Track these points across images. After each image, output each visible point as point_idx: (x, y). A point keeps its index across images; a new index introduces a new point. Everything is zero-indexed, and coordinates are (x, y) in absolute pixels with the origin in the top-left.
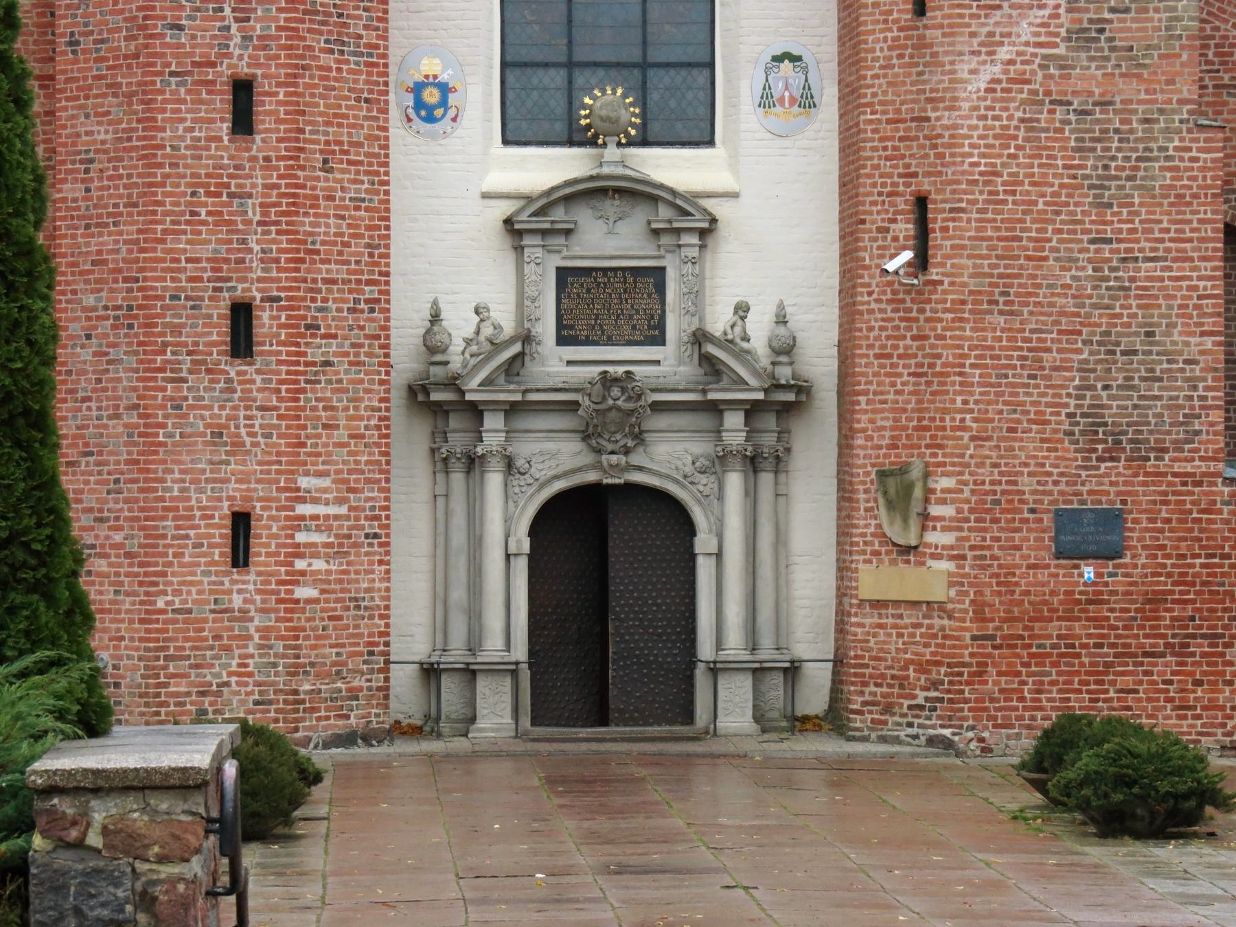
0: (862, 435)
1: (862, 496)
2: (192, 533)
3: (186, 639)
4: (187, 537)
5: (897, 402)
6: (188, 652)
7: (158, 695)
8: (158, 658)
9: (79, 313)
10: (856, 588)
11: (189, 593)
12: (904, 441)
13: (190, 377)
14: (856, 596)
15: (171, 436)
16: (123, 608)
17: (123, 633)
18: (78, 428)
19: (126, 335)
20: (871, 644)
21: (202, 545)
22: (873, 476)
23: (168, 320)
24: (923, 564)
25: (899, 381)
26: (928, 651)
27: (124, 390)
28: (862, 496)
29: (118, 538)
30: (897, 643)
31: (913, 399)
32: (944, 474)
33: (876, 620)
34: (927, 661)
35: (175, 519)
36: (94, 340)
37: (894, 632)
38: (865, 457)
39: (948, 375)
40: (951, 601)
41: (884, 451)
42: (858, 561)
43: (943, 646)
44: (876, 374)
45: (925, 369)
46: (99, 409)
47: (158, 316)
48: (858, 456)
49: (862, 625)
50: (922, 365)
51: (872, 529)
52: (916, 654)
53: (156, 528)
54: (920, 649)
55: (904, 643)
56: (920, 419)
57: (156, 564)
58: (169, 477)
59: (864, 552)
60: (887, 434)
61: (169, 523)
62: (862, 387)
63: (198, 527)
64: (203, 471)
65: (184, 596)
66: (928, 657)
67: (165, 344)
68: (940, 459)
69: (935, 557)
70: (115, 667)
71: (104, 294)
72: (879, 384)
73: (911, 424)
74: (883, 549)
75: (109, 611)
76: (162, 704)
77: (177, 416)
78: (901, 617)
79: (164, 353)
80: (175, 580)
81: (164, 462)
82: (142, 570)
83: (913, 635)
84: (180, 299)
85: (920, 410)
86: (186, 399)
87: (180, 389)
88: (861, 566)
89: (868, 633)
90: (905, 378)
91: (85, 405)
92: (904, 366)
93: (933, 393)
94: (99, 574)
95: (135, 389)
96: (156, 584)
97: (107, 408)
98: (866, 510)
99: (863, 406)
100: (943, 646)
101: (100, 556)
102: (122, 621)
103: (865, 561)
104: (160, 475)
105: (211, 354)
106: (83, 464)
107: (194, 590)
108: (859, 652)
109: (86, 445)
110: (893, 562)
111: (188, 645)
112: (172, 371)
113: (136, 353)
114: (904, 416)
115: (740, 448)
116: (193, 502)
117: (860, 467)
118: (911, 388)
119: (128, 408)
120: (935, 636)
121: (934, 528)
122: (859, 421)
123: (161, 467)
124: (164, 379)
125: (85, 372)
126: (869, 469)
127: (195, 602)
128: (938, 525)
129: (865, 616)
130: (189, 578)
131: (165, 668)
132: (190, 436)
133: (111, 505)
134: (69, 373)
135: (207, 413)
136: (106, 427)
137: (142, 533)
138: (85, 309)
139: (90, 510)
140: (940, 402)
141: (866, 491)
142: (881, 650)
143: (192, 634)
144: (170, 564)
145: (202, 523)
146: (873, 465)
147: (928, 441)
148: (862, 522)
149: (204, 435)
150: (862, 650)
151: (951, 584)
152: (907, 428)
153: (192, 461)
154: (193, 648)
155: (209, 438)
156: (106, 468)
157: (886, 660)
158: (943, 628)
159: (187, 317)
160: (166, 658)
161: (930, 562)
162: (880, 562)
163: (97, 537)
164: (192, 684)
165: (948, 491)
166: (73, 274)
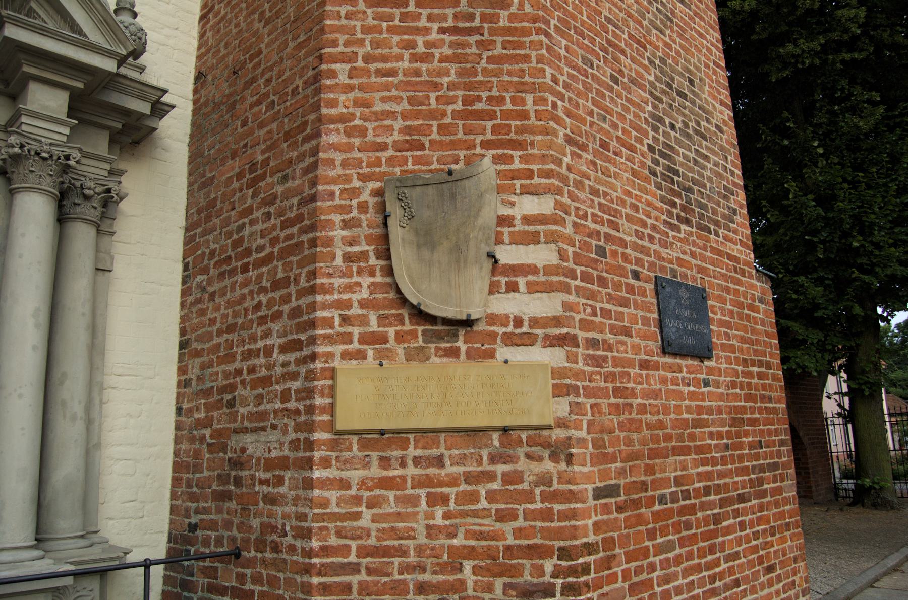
0: (341, 126)
1: (339, 233)
5: (418, 73)
10: (331, 409)
12: (435, 136)
14: (331, 426)
20: (365, 522)
22: (365, 196)
24: (491, 354)
25: (420, 40)
26: (508, 528)
28: (339, 233)
30: (430, 516)
31: (453, 68)
32: (527, 191)
33: (376, 471)
34: (508, 548)
37: (422, 492)
38: (345, 164)
39: (526, 32)
40: (562, 423)
41: (390, 152)
42: (330, 356)
43: (546, 515)
44: (366, 30)
45: (477, 23)
48: (331, 162)
49: (344, 484)
50: (471, 17)
51: (365, 294)
52: (480, 536)
54: (488, 524)
55: (446, 516)
56: (467, 101)
59: (347, 338)
60: (398, 124)
62: (341, 49)
66: (511, 541)
68: (517, 165)
69: (511, 340)
72: (376, 44)
73: (450, 109)
74: (391, 332)
78: (439, 462)
83: (473, 497)
85: (468, 87)
88: (337, 363)
89: (357, 500)
90: (434, 36)
92: (430, 18)
93: (490, 60)
98: (348, 258)
99: (343, 79)
100: (546, 515)
103: (346, 355)
108: (333, 541)
110: (416, 355)
114: (433, 95)
115: (56, 151)
117: (334, 181)
118: (447, 51)
120: (528, 497)
121: (512, 288)
122: (333, 104)
126: (356, 183)
128: (522, 281)
129: (347, 464)
140: (510, 73)
141: (346, 224)
142: (394, 533)
146: (364, 178)
147: (489, 136)
148: (338, 282)
150: (339, 534)
151: (560, 391)
152: (444, 114)
157: (403, 552)
158: (544, 480)
161: (503, 352)
162: (383, 357)
165: (542, 219)
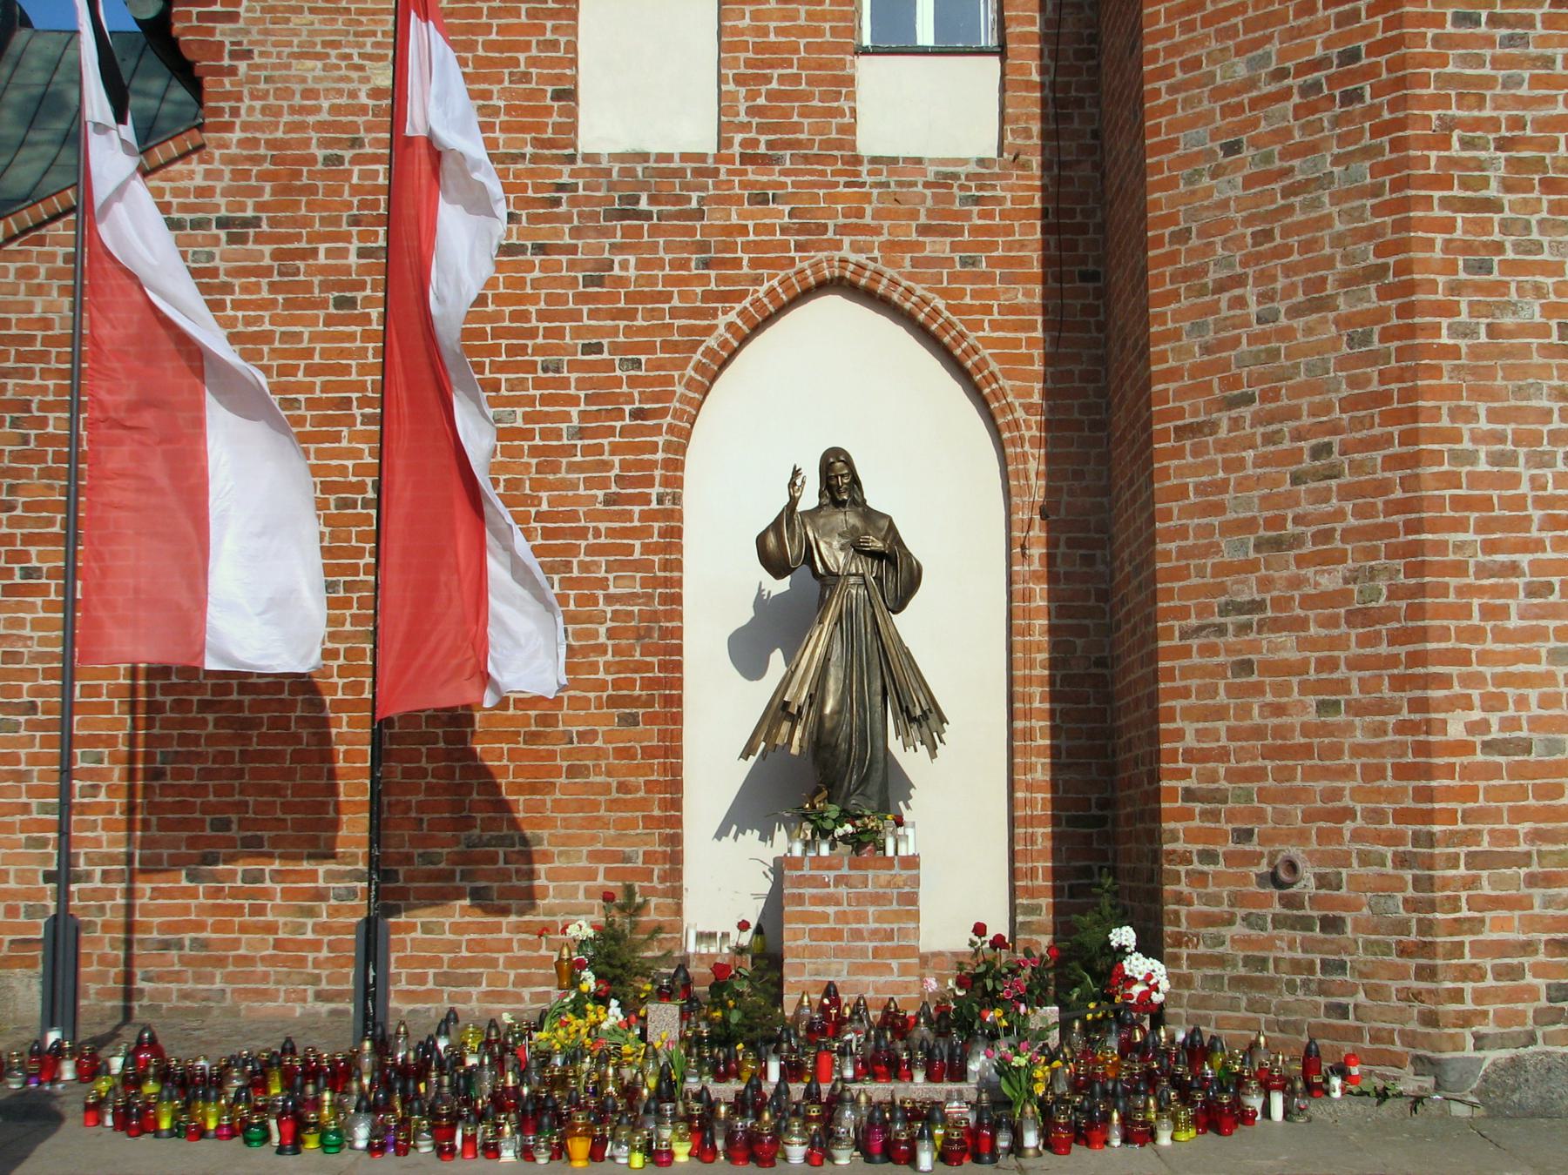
2: (1524, 559)
3: (1519, 815)
4: (1514, 569)
6: (1523, 847)
7: (1457, 950)
8: (1453, 861)
9: (1206, 105)
11: (1522, 702)
13: (1507, 198)
15: (1468, 332)
16: (1347, 742)
17: (1347, 802)
18: (1207, 349)
19: (1336, 122)
21: (1549, 588)
23: (1450, 69)
27: (1338, 240)
29: (1329, 580)
35: (1483, 527)
36: (1248, 153)
46: (1264, 297)
47: (1427, 60)
53: (1441, 547)
57: (1444, 634)
58: (1465, 429)
61: (1469, 536)
63: (1539, 545)
64: (1546, 415)
65: (1511, 712)
67: (1449, 125)
70: (1322, 881)
71: (1273, 47)
75: (1307, 751)
76: (1465, 973)
77: (1478, 288)
79: (1445, 143)
80: (1488, 671)
81: (1455, 392)
82: (1402, 650)
84: (1478, 23)
86: (1499, 248)
87: (1485, 227)
91: (1225, 297)
94: (1270, 668)
95: (1371, 233)
96: (1445, 681)
97: (1289, 291)
101: (1276, 625)
102: (1347, 772)
104: (1445, 422)
105: (1555, 147)
106: (1225, 425)
107: (1533, 695)
109: (1235, 382)
111: (1524, 827)
112: (1464, 185)
113: (1367, 152)
116: (1525, 488)
119: (1347, 281)
123: (1445, 406)
124: (1446, 203)
125: (1224, 226)
127: (1535, 723)
130: (1521, 668)
131: (1472, 883)
132: (1511, 334)
133: (1305, 507)
134: (1182, 236)
135: (1549, 281)
136: (1286, 334)
137: (1399, 563)
138: (1219, 93)
139: (1248, 525)
143: (1531, 802)
144: (1476, 634)
145: (1547, 535)
149: (1544, 331)
153: (1519, 392)
154: (1536, 836)
155: (1555, 339)
156: (1287, 427)
159: (1496, 63)
160: (1474, 860)
163: (1265, 584)
164: (1531, 923)
166: (1189, 27)
